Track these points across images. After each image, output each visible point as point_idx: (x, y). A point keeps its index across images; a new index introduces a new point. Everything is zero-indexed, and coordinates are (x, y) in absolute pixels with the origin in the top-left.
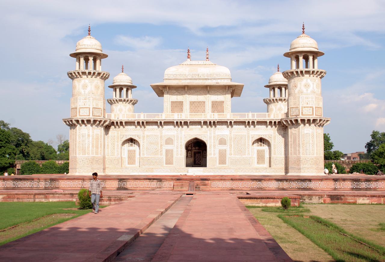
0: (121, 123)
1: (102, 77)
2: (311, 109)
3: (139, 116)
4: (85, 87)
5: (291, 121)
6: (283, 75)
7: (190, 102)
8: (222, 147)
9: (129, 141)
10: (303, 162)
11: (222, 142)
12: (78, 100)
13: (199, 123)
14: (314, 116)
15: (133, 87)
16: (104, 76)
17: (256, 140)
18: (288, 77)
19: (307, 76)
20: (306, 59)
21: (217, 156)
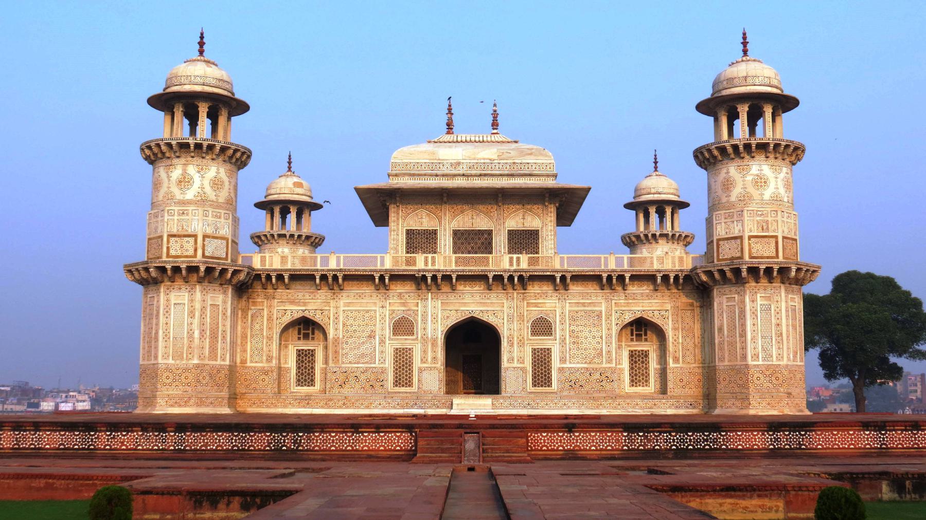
0: (280, 277)
1: (231, 158)
2: (773, 240)
3: (325, 261)
4: (185, 182)
5: (722, 272)
6: (696, 157)
7: (455, 233)
8: (543, 342)
9: (299, 324)
10: (755, 378)
11: (542, 327)
12: (166, 214)
13: (481, 278)
14: (781, 259)
15: (317, 207)
16: (238, 155)
17: (625, 326)
18: (712, 160)
19: (760, 157)
20: (754, 118)
21: (528, 365)
